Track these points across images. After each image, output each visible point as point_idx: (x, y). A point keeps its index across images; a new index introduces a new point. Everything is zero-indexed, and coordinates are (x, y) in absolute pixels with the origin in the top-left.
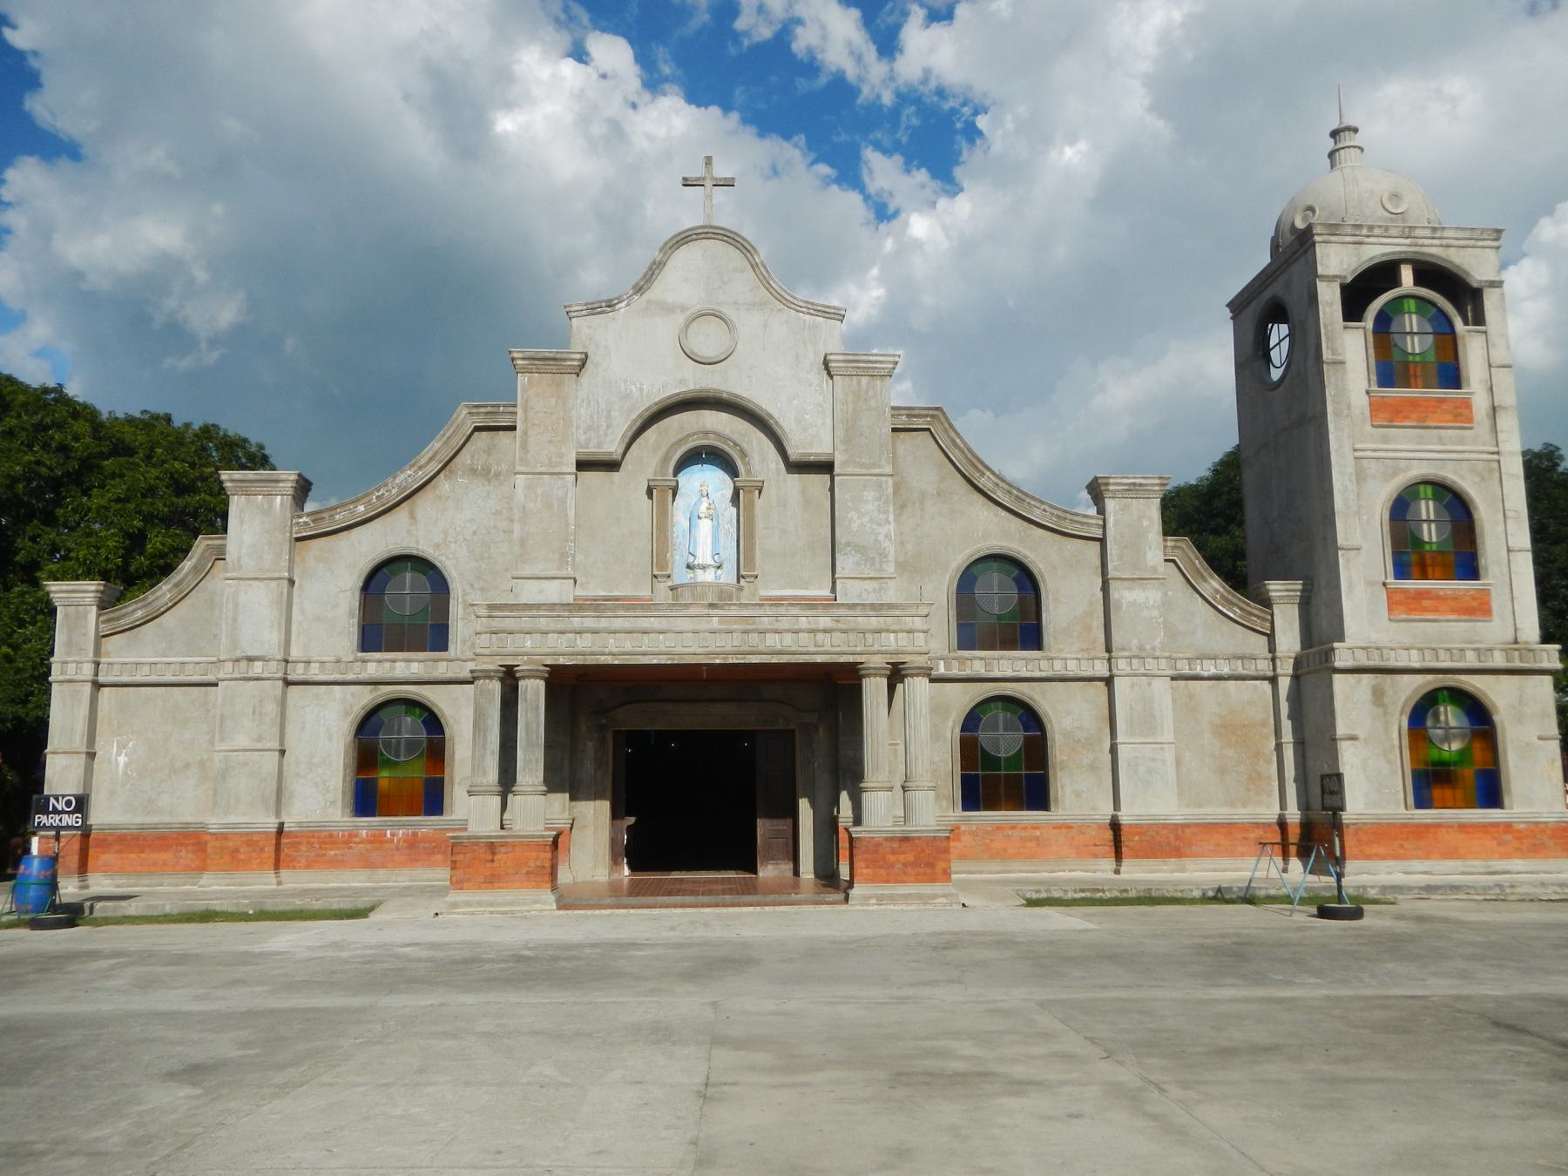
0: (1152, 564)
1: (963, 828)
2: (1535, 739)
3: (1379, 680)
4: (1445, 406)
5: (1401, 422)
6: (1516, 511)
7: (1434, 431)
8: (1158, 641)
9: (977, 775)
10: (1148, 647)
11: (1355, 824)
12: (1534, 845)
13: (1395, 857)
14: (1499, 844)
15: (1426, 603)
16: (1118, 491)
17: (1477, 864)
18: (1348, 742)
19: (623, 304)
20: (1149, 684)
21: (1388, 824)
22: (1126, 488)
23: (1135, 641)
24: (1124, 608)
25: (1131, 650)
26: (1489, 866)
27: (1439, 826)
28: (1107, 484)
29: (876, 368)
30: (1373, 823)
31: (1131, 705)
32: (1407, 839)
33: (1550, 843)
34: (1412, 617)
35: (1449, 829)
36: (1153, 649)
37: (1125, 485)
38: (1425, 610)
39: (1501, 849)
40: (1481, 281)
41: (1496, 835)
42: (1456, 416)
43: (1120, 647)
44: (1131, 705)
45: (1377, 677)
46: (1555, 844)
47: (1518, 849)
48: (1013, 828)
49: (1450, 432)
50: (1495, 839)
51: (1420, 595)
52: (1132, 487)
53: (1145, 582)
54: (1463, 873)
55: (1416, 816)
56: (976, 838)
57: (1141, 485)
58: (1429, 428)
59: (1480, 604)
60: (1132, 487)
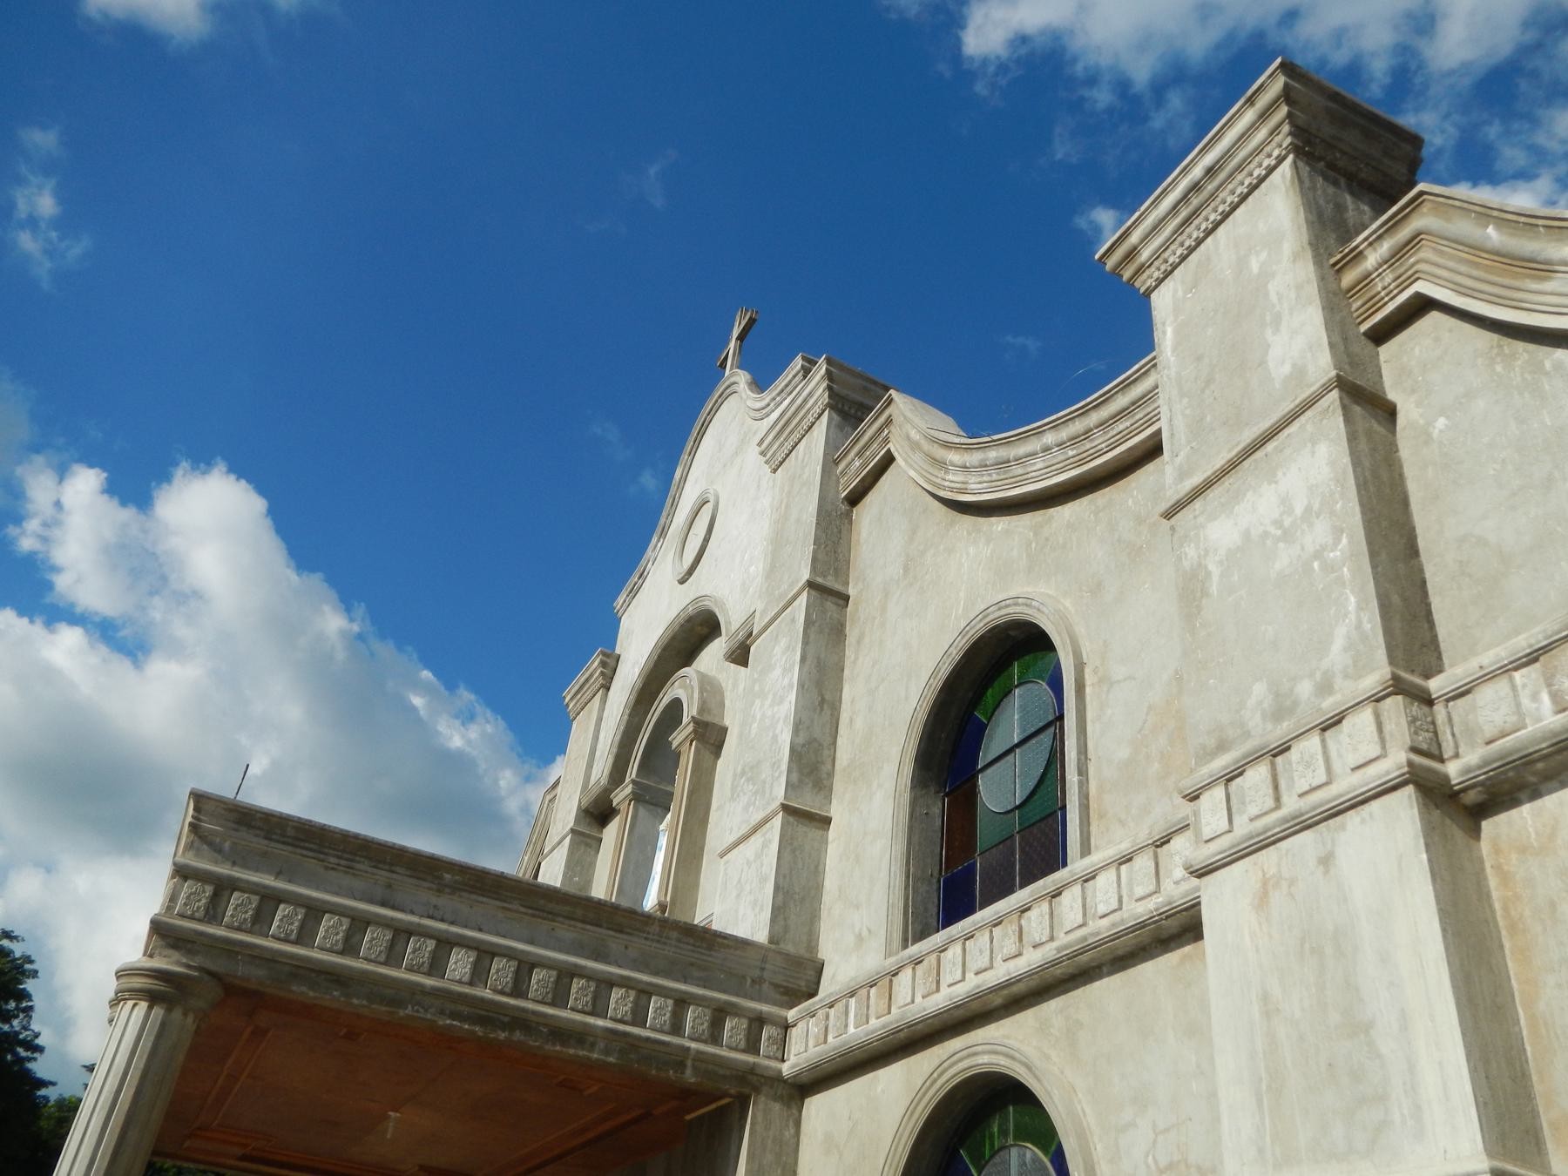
0: (1287, 369)
8: (1338, 643)
10: (1305, 689)
16: (1165, 246)
19: (649, 565)
20: (1326, 861)
23: (1259, 690)
24: (1214, 589)
25: (1247, 735)
31: (1265, 998)
36: (1325, 688)
37: (1175, 208)
43: (1211, 742)
44: (1265, 998)
53: (1270, 447)
57: (1211, 172)
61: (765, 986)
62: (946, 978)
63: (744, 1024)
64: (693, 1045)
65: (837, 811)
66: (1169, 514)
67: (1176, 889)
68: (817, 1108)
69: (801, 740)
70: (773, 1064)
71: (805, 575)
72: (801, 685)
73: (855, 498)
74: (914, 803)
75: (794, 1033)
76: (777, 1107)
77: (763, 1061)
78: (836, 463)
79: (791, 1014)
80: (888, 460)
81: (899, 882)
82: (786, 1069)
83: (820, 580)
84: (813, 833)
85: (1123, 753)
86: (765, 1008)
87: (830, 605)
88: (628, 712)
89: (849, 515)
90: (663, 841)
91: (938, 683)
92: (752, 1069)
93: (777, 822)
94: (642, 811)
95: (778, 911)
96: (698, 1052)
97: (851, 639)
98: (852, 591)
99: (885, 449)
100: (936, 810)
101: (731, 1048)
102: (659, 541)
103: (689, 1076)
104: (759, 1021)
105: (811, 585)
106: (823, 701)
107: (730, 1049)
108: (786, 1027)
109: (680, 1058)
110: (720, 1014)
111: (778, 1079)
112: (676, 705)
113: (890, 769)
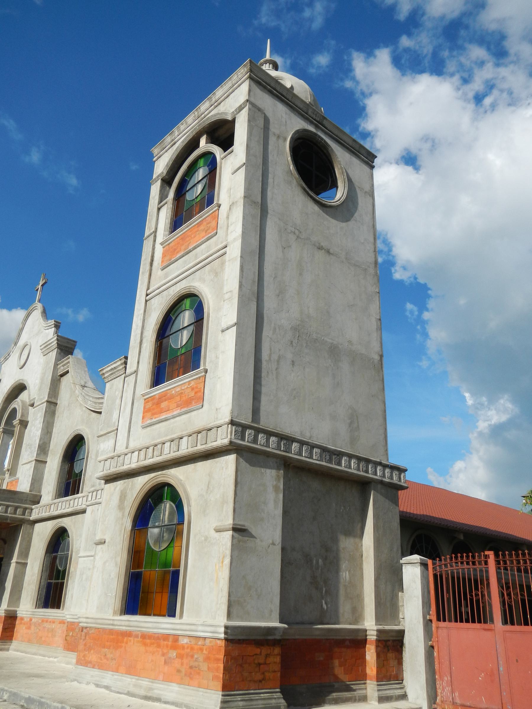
1: (33, 620)
2: (213, 532)
3: (125, 484)
4: (202, 227)
5: (176, 256)
6: (230, 291)
7: (194, 251)
9: (58, 582)
11: (86, 628)
12: (191, 667)
13: (101, 667)
14: (165, 663)
15: (164, 405)
17: (145, 683)
18: (100, 547)
19: (11, 353)
21: (104, 629)
22: (110, 373)
26: (151, 689)
27: (128, 634)
28: (103, 374)
29: (52, 346)
30: (96, 628)
32: (109, 648)
33: (204, 667)
34: (154, 420)
35: (136, 639)
38: (161, 412)
39: (166, 669)
40: (233, 112)
41: (165, 651)
42: (206, 231)
45: (125, 483)
46: (209, 668)
47: (179, 671)
48: (47, 621)
49: (203, 246)
50: (163, 655)
51: (163, 397)
52: (113, 371)
54: (129, 694)
55: (115, 623)
56: (36, 628)
57: (115, 368)
58: (190, 251)
59: (196, 393)
60: (113, 371)
61: (28, 501)
62: (59, 508)
63: (22, 510)
64: (10, 515)
65: (49, 460)
66: (98, 437)
67: (84, 507)
68: (37, 526)
69: (41, 443)
70: (28, 517)
71: (46, 399)
72: (42, 429)
73: (62, 376)
74: (61, 466)
75: (34, 511)
76: (28, 526)
77: (26, 517)
78: (58, 365)
79: (33, 507)
80: (67, 372)
81: (56, 483)
82: (31, 518)
83: (50, 400)
84: (43, 465)
85: (90, 474)
86: (27, 506)
87: (52, 406)
88: (2, 403)
89: (60, 380)
90: (11, 446)
91: (69, 440)
92: (23, 519)
93: (34, 462)
94: (5, 436)
95: (32, 484)
96: (11, 517)
97: (56, 416)
98: (58, 402)
99: (67, 369)
100: (67, 467)
101: (19, 515)
102: (14, 346)
103: (9, 521)
104: (25, 509)
105: (47, 401)
106: (48, 432)
107: (18, 515)
108: (32, 509)
109: (7, 518)
110: (16, 508)
111: (29, 521)
112: (14, 411)
113: (59, 455)
